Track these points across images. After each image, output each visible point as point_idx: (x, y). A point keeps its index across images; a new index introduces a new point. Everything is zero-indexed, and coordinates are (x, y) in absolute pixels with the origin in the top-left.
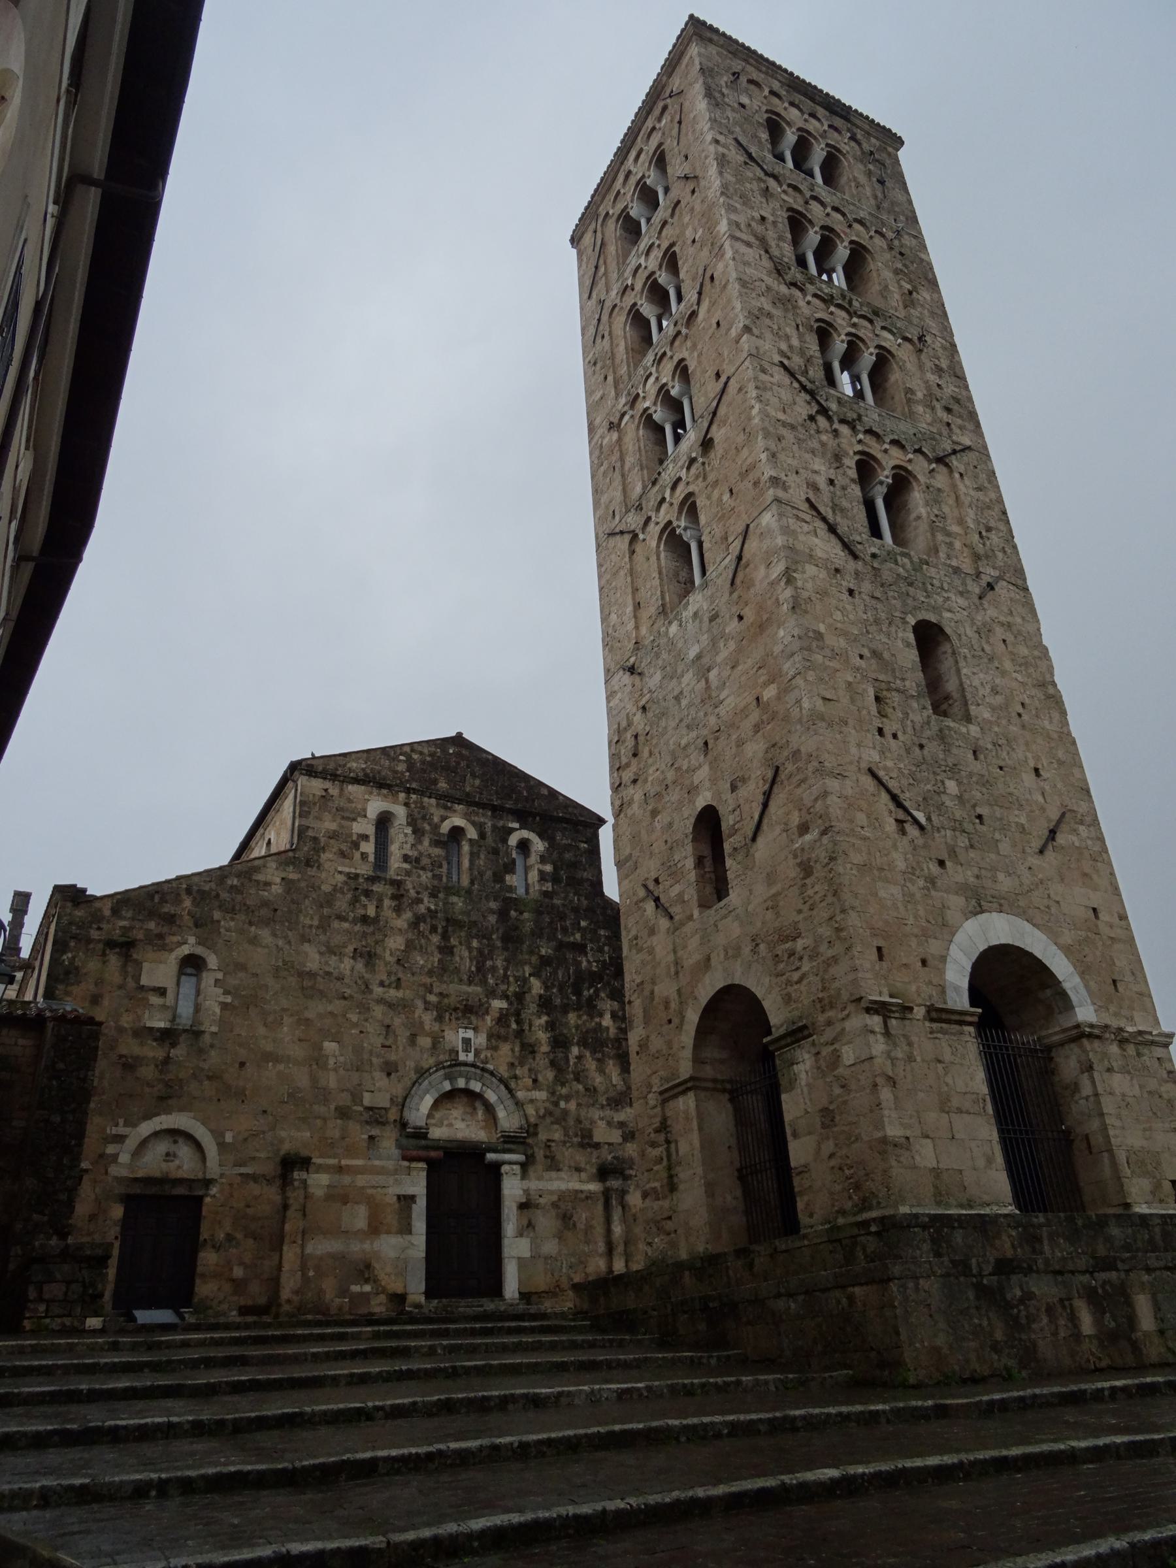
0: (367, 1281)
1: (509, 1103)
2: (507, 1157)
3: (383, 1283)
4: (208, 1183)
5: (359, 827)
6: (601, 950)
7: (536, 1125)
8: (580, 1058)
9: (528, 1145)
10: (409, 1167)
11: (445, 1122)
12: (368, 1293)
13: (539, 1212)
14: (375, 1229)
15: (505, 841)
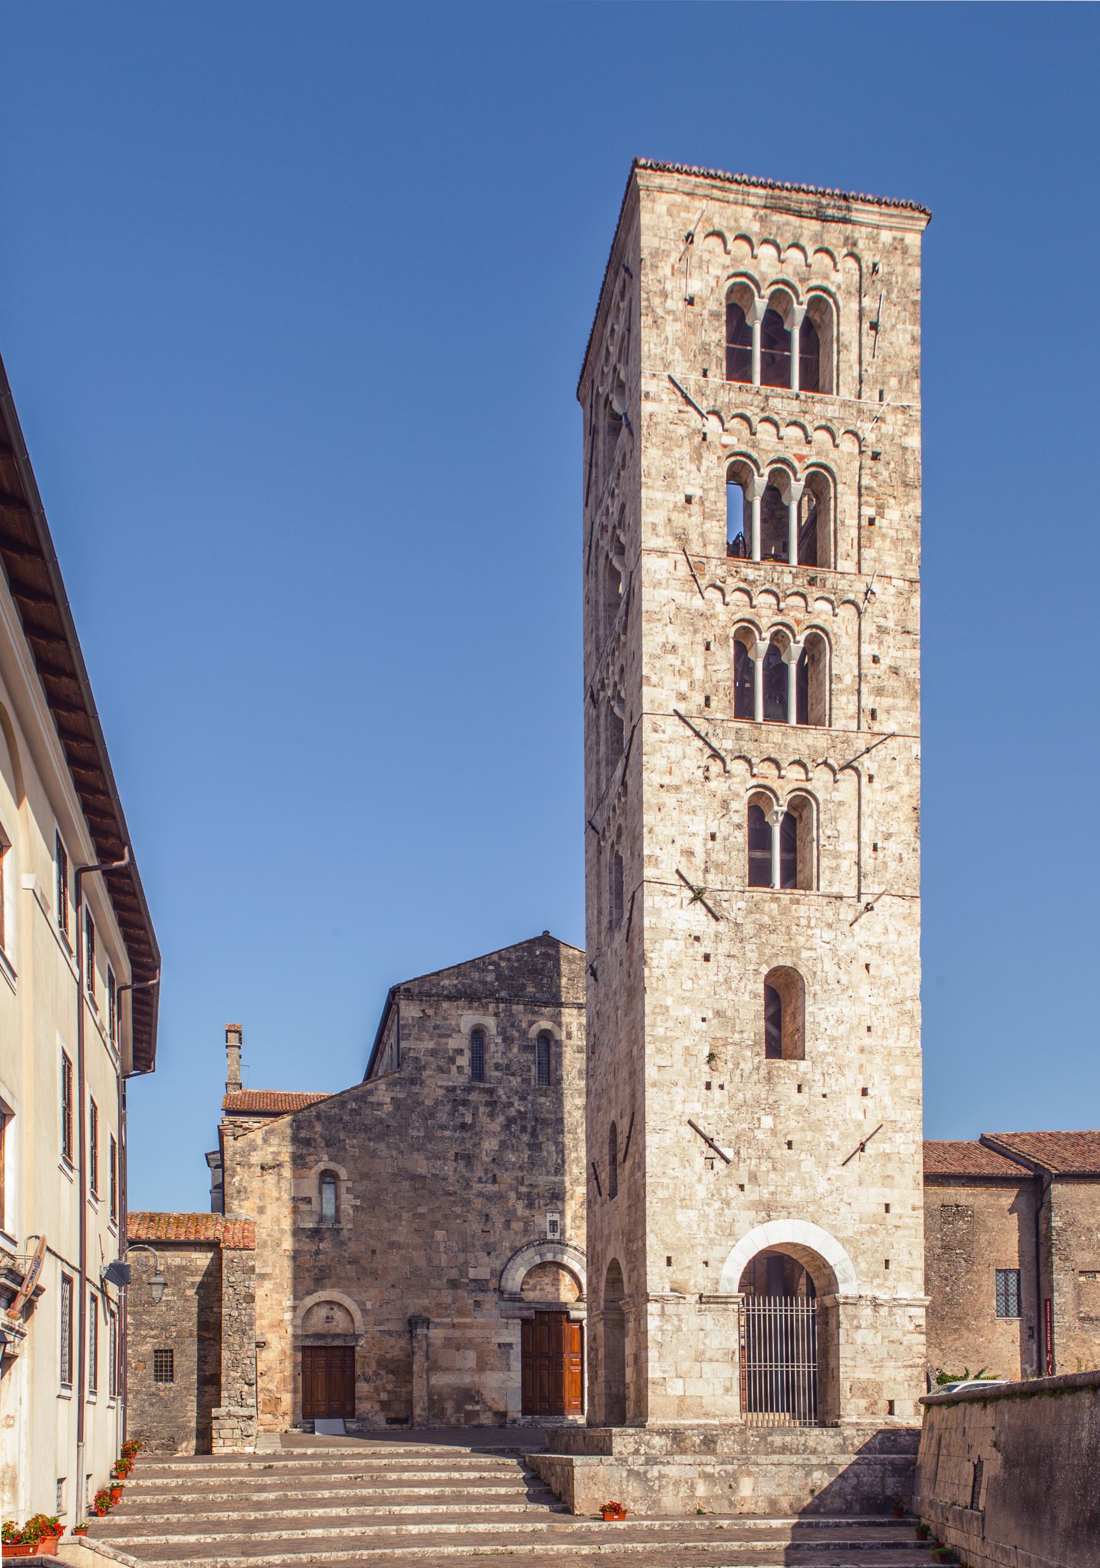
5: (453, 1043)
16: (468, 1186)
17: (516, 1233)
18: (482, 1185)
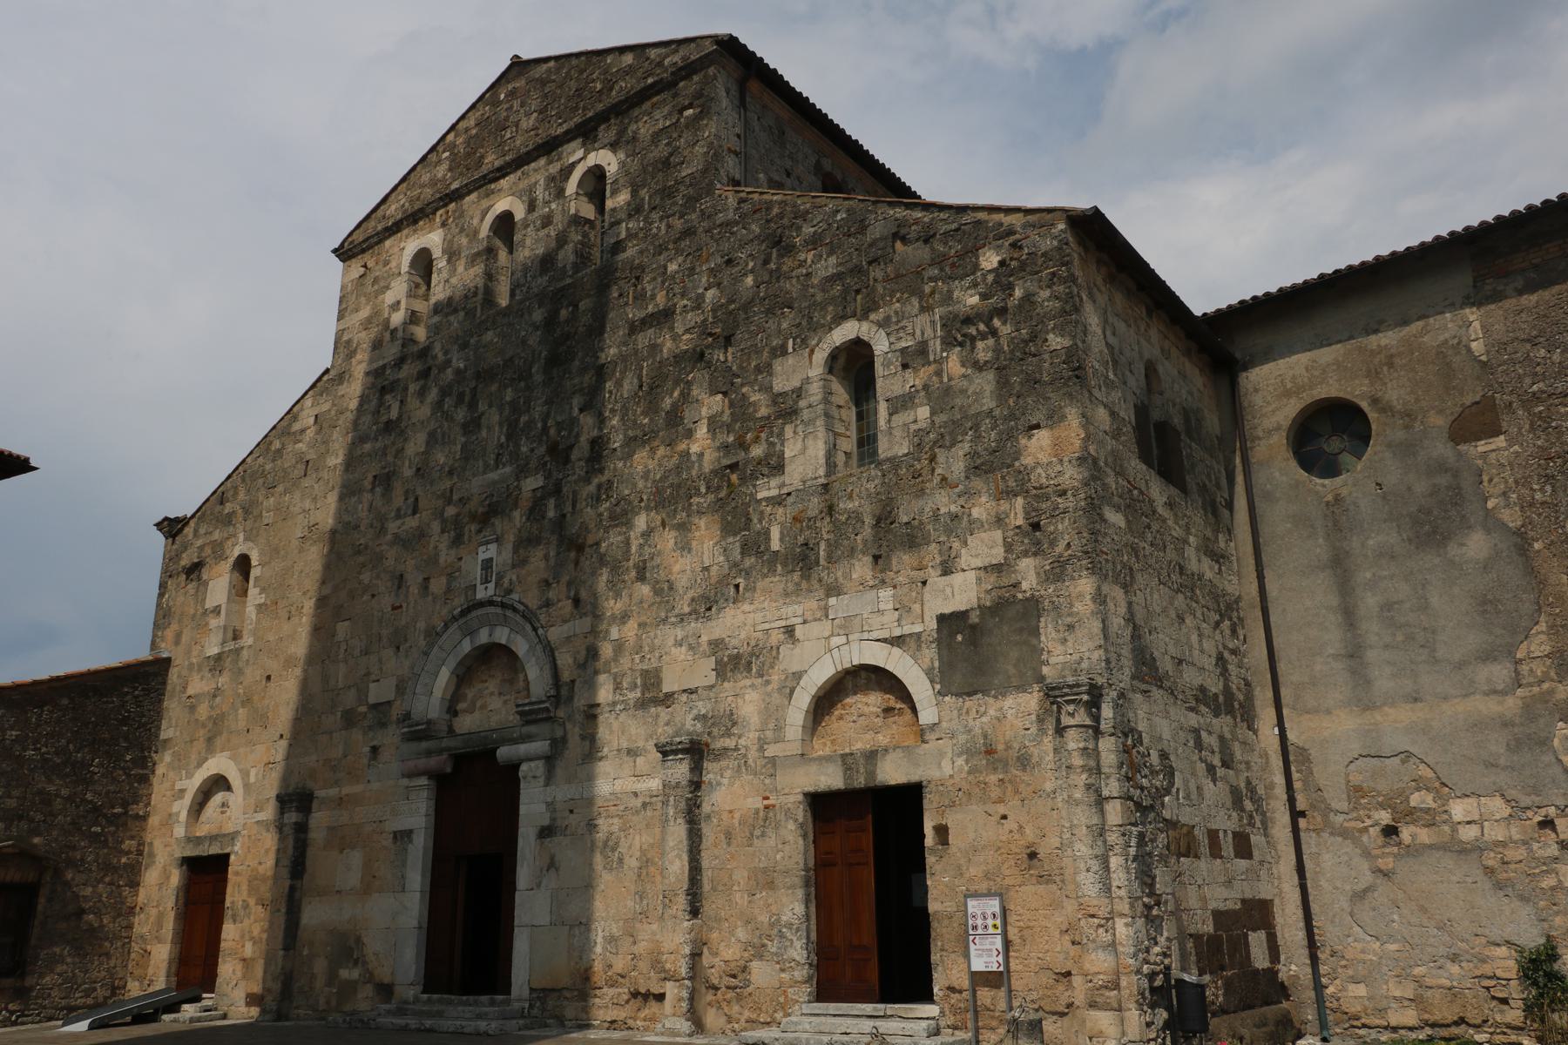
0: (356, 962)
2: (523, 749)
3: (370, 967)
4: (233, 837)
6: (698, 303)
8: (647, 534)
11: (478, 704)
12: (356, 982)
14: (367, 888)
15: (560, 193)
16: (383, 530)
18: (398, 522)
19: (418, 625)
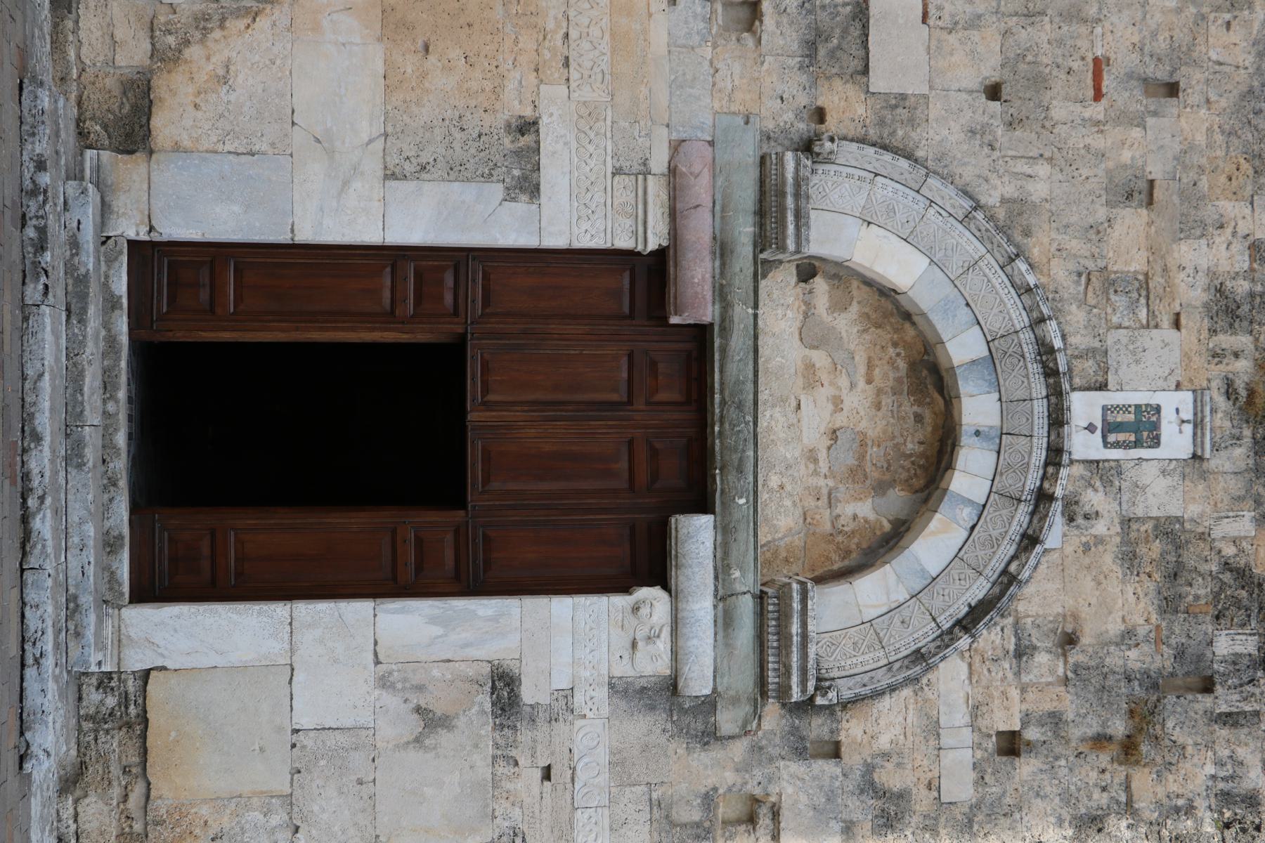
1: (922, 633)
2: (702, 607)
3: (194, 52)
7: (835, 752)
9: (757, 714)
10: (646, 173)
11: (820, 358)
13: (484, 770)
17: (1096, 232)
19: (1043, 169)
